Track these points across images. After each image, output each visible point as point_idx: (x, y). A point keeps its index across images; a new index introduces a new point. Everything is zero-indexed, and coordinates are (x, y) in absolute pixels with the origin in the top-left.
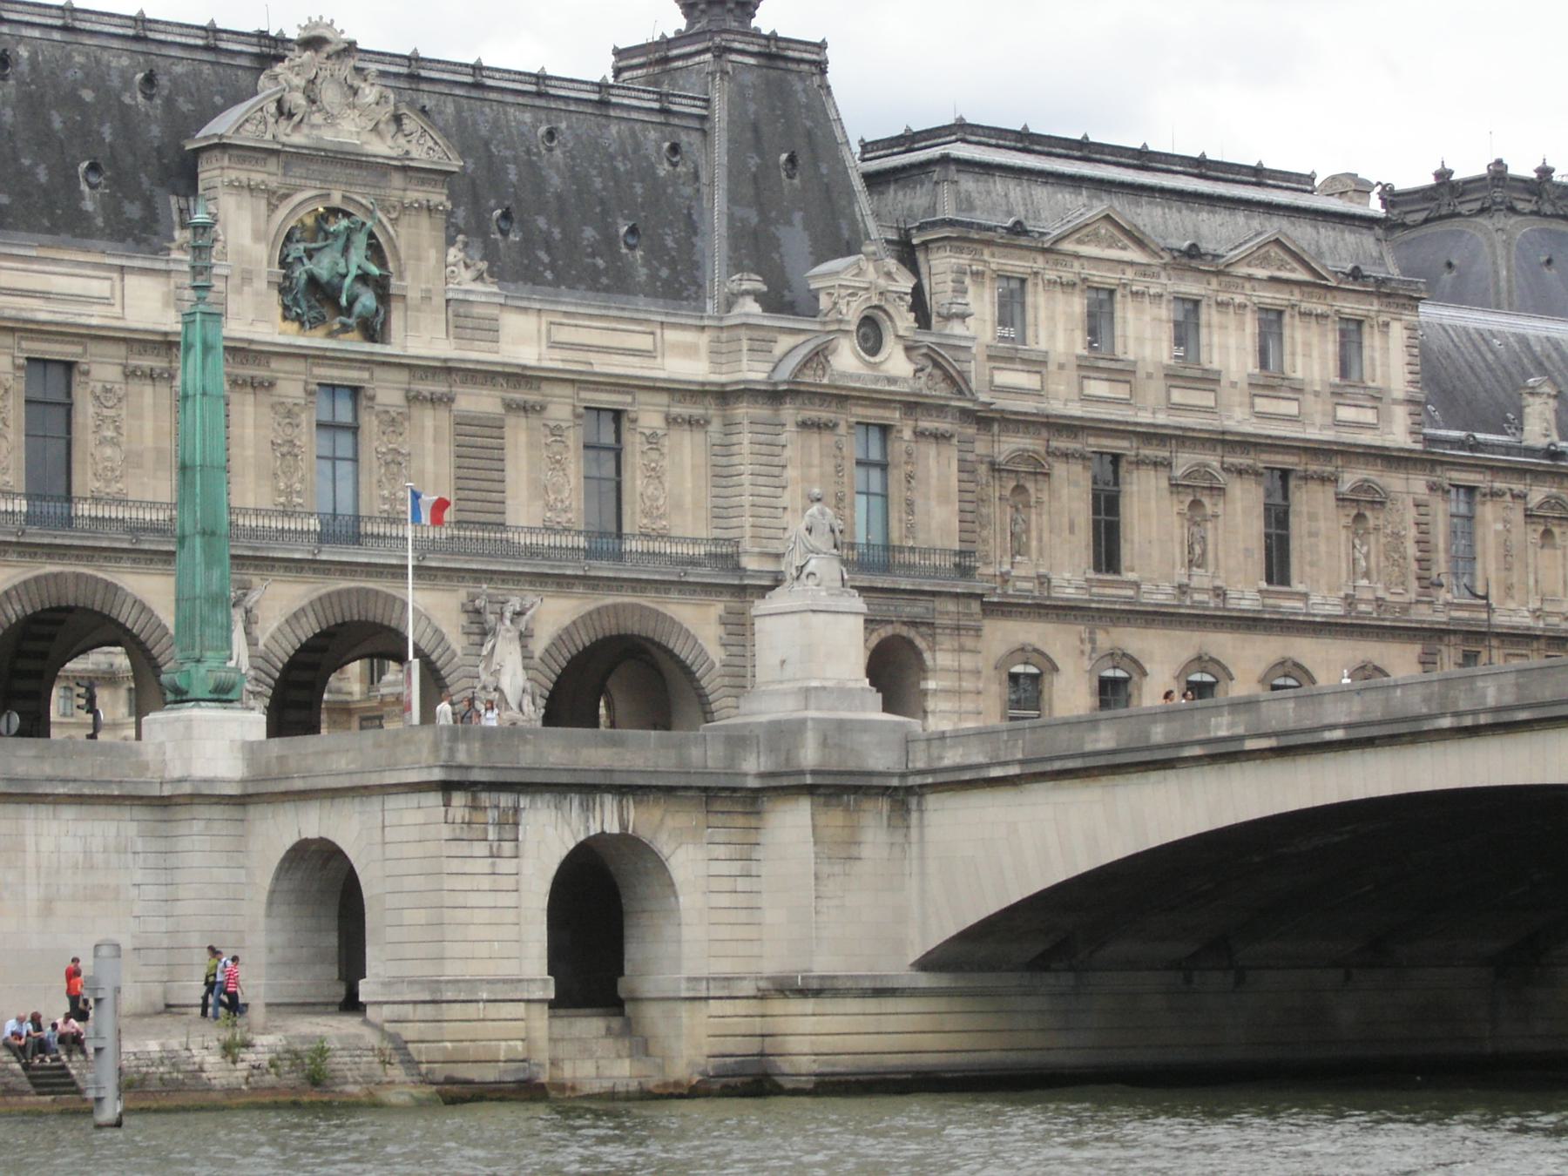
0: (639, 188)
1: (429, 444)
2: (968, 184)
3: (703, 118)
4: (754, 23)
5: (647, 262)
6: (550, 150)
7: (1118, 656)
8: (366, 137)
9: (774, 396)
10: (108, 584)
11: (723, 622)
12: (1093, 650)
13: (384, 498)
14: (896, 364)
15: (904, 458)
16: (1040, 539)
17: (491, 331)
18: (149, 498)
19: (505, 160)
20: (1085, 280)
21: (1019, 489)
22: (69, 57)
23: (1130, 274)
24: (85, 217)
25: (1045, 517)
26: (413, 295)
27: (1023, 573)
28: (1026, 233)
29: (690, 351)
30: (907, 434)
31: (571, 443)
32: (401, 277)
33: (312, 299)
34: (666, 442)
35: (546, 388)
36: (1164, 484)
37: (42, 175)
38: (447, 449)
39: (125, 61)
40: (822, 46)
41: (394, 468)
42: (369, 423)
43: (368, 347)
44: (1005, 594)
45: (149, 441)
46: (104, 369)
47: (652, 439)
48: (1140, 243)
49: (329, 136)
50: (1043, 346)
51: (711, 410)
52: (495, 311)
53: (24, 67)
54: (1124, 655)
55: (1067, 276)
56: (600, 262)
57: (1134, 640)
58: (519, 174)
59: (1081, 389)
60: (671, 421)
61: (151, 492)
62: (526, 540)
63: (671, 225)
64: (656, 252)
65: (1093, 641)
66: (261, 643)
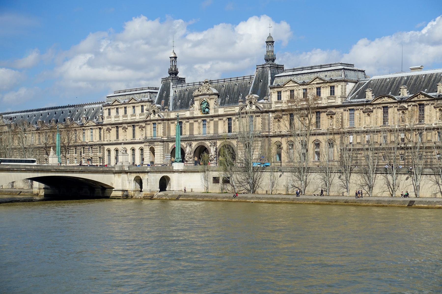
23: (295, 87)
42: (207, 123)
46: (184, 122)
48: (296, 83)
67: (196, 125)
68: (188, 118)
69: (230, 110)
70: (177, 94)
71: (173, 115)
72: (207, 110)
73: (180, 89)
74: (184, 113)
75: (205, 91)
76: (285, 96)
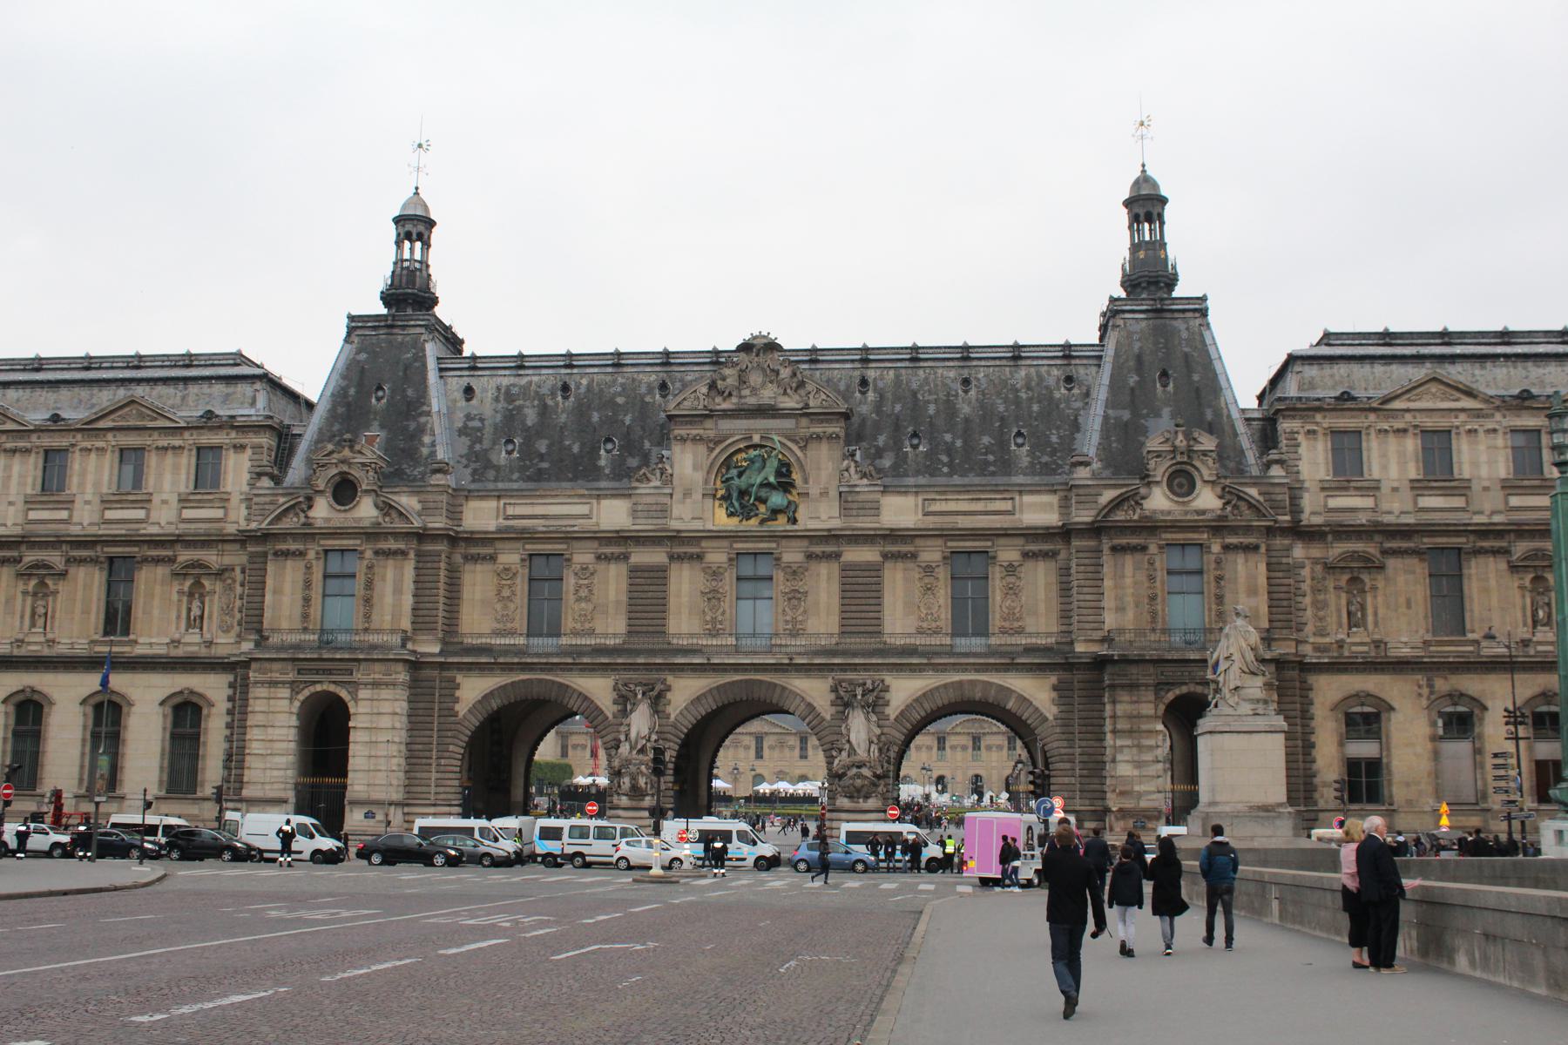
0: (1035, 408)
1: (823, 584)
2: (1311, 371)
3: (1100, 357)
4: (1174, 295)
5: (1031, 453)
6: (966, 392)
7: (1456, 696)
8: (781, 399)
9: (1096, 530)
10: (561, 684)
11: (1055, 688)
12: (1432, 693)
13: (787, 622)
14: (1207, 500)
15: (1213, 566)
16: (1376, 614)
17: (876, 509)
18: (610, 631)
19: (928, 402)
20: (1416, 427)
21: (1354, 580)
22: (615, 381)
23: (1462, 417)
24: (599, 469)
25: (1380, 599)
26: (814, 490)
27: (1357, 640)
28: (1354, 399)
29: (1045, 507)
30: (1216, 548)
31: (941, 576)
32: (806, 481)
33: (741, 501)
34: (1023, 569)
35: (919, 542)
36: (1503, 565)
37: (576, 449)
38: (836, 587)
39: (654, 377)
40: (1203, 299)
41: (795, 602)
42: (779, 576)
43: (789, 527)
44: (1341, 656)
45: (612, 596)
46: (583, 556)
47: (1011, 569)
48: (1470, 393)
49: (752, 401)
50: (1376, 475)
51: (1058, 546)
52: (878, 496)
53: (583, 390)
54: (1462, 695)
55: (1399, 425)
56: (991, 458)
57: (1471, 684)
58: (938, 411)
59: (1416, 503)
60: (1026, 555)
61: (613, 627)
62: (900, 642)
63: (1058, 428)
64: (1040, 444)
65: (1430, 686)
66: (672, 717)
67: (684, 584)
68: (621, 538)
69: (979, 506)
70: (486, 404)
71: (481, 516)
72: (777, 499)
73: (505, 382)
74: (582, 509)
75: (768, 395)
76: (1392, 462)
